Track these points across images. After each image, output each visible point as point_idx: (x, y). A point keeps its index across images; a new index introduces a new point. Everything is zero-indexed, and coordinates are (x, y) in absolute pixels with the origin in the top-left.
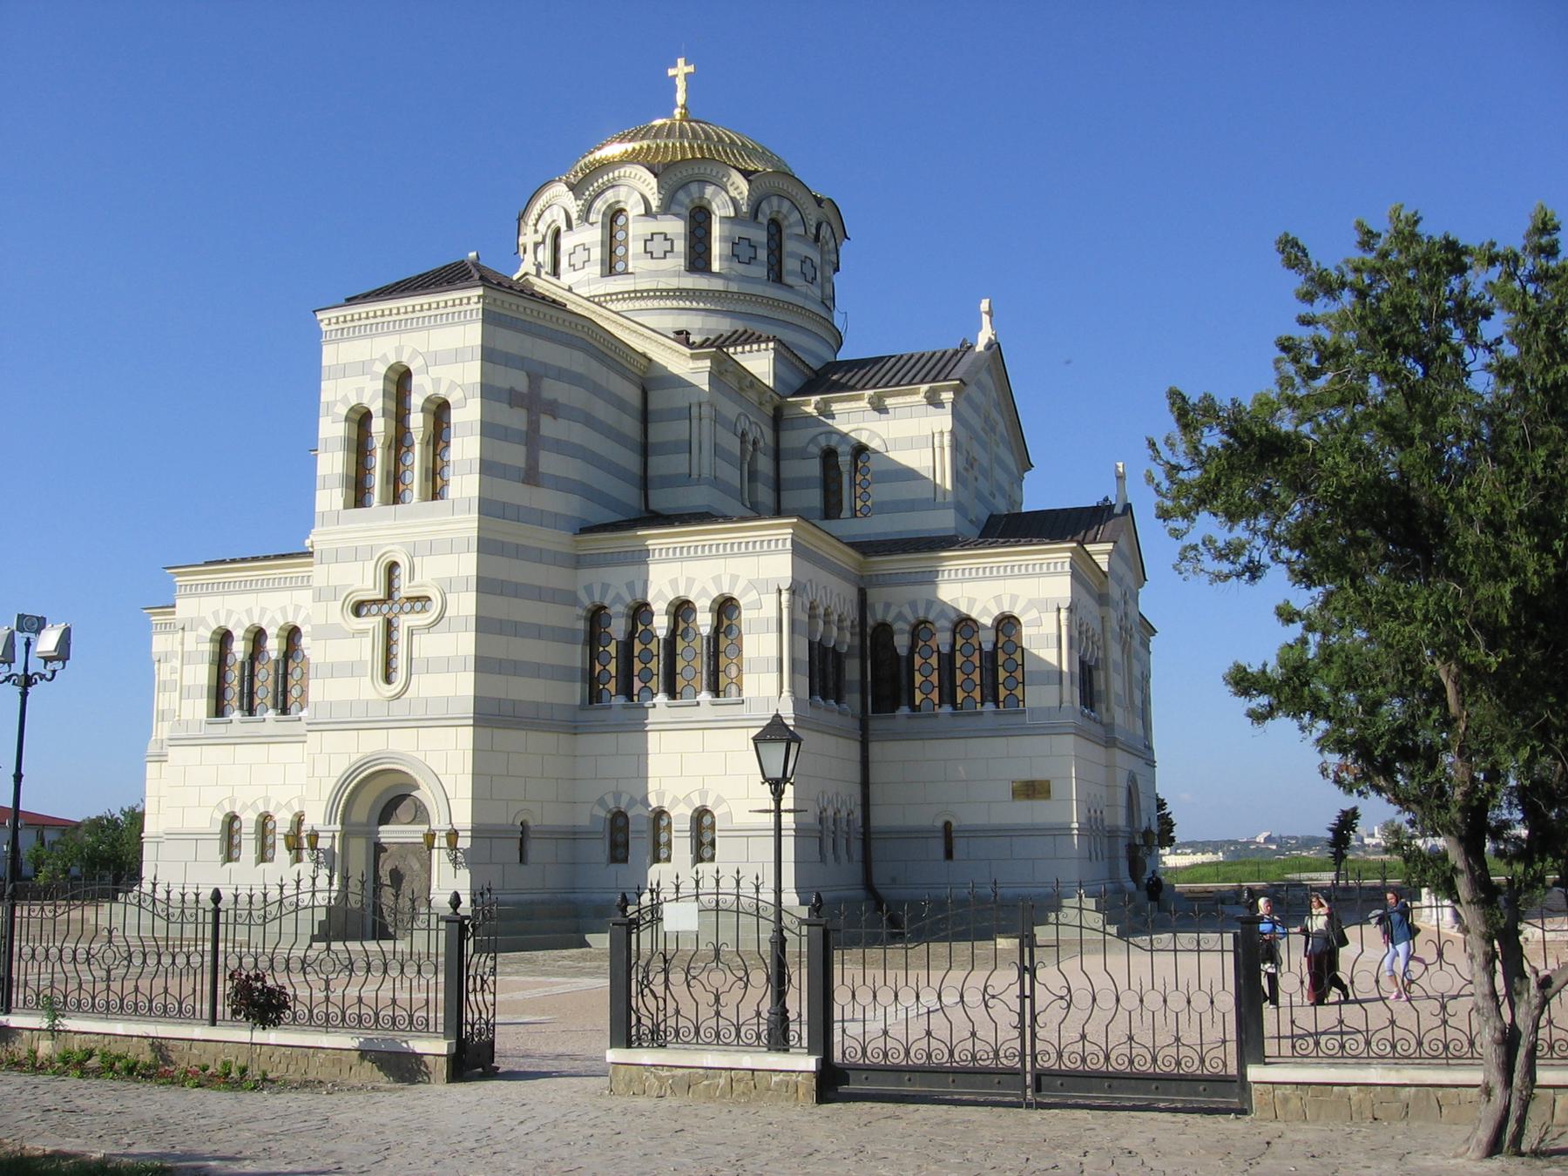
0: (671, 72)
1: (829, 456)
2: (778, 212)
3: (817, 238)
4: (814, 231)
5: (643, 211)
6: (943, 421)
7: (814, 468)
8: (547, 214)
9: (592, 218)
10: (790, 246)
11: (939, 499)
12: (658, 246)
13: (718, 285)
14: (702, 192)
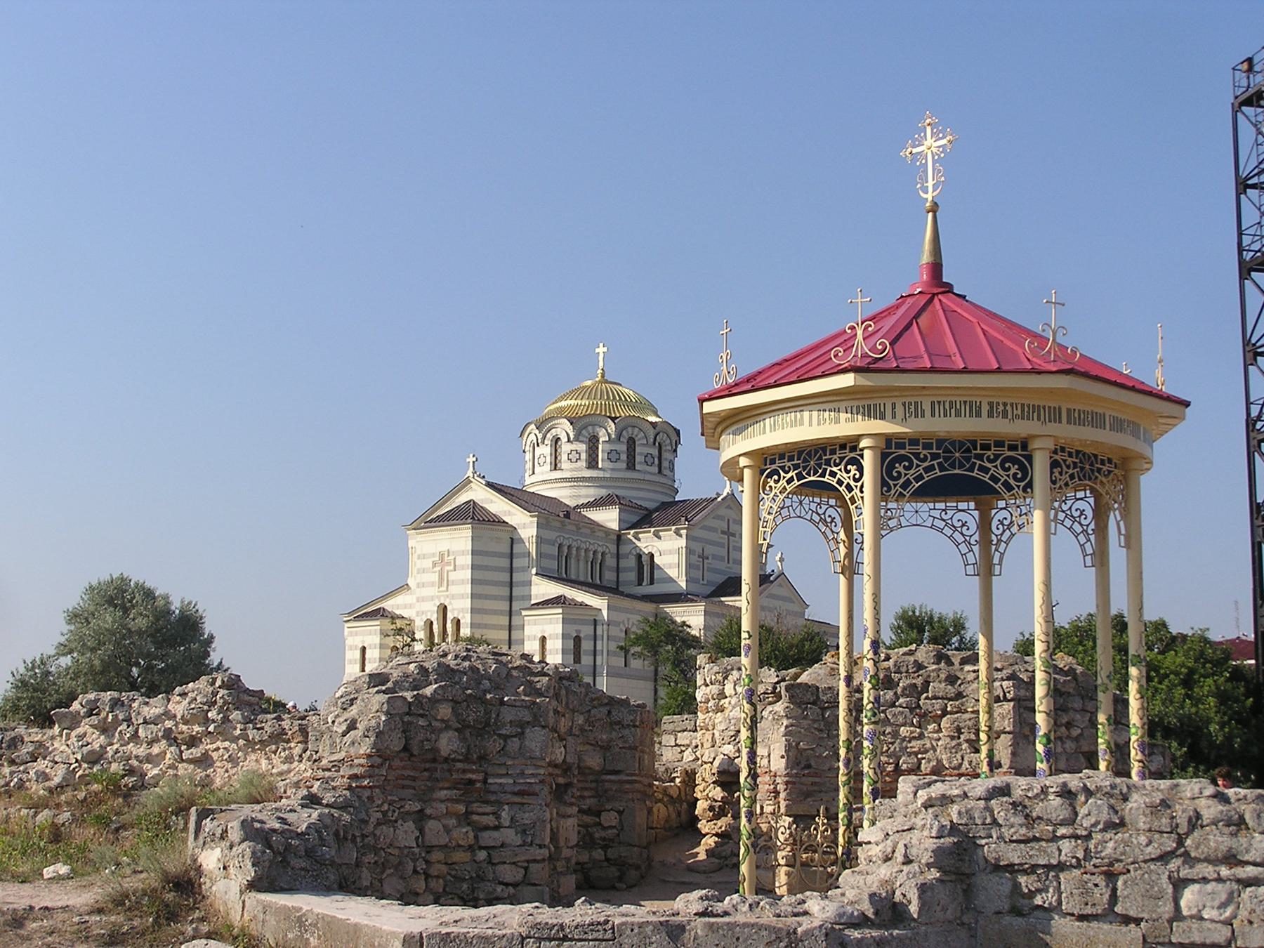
0: (597, 350)
1: (639, 557)
4: (652, 440)
6: (682, 542)
7: (632, 562)
9: (546, 442)
10: (638, 450)
12: (574, 456)
13: (601, 474)
14: (593, 429)
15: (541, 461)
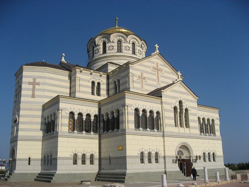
12: (128, 48)
15: (111, 48)
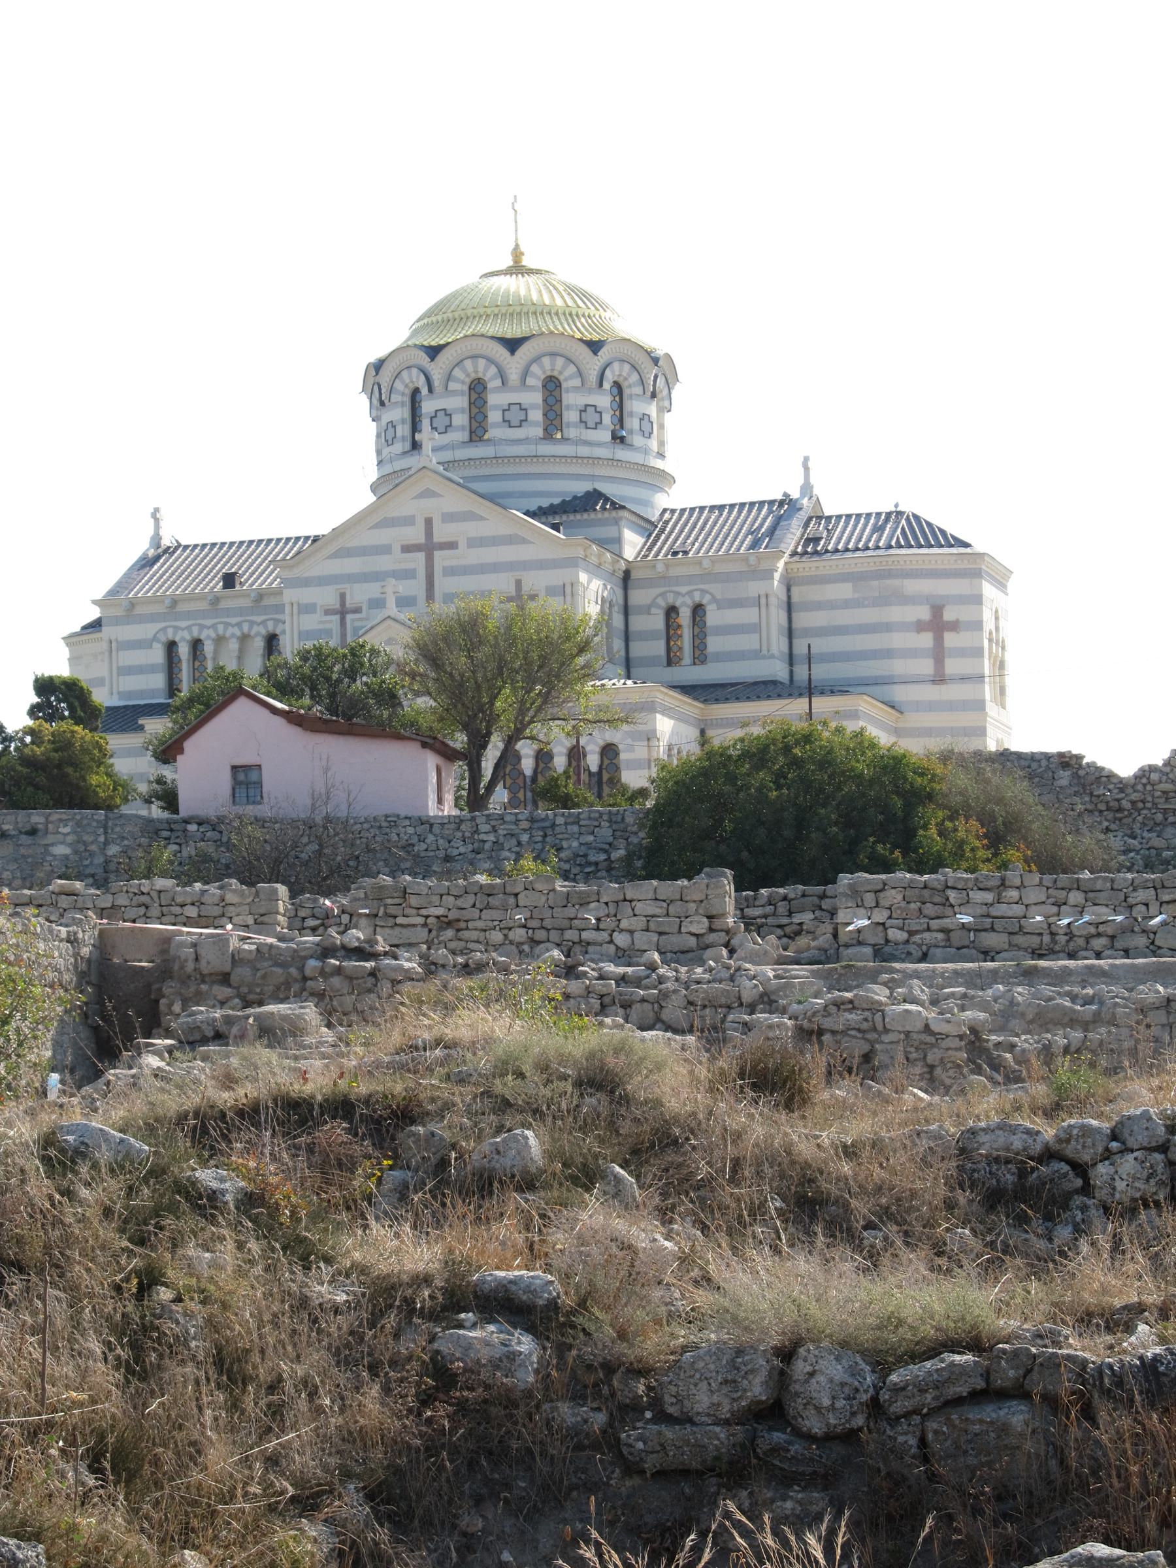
2: (620, 375)
3: (654, 395)
5: (498, 383)
8: (405, 374)
9: (453, 386)
11: (765, 652)
12: (515, 416)
14: (553, 364)
15: (441, 421)
